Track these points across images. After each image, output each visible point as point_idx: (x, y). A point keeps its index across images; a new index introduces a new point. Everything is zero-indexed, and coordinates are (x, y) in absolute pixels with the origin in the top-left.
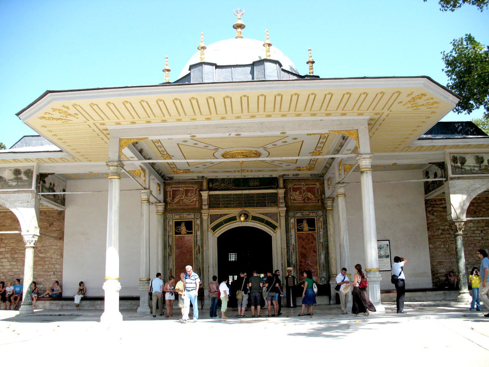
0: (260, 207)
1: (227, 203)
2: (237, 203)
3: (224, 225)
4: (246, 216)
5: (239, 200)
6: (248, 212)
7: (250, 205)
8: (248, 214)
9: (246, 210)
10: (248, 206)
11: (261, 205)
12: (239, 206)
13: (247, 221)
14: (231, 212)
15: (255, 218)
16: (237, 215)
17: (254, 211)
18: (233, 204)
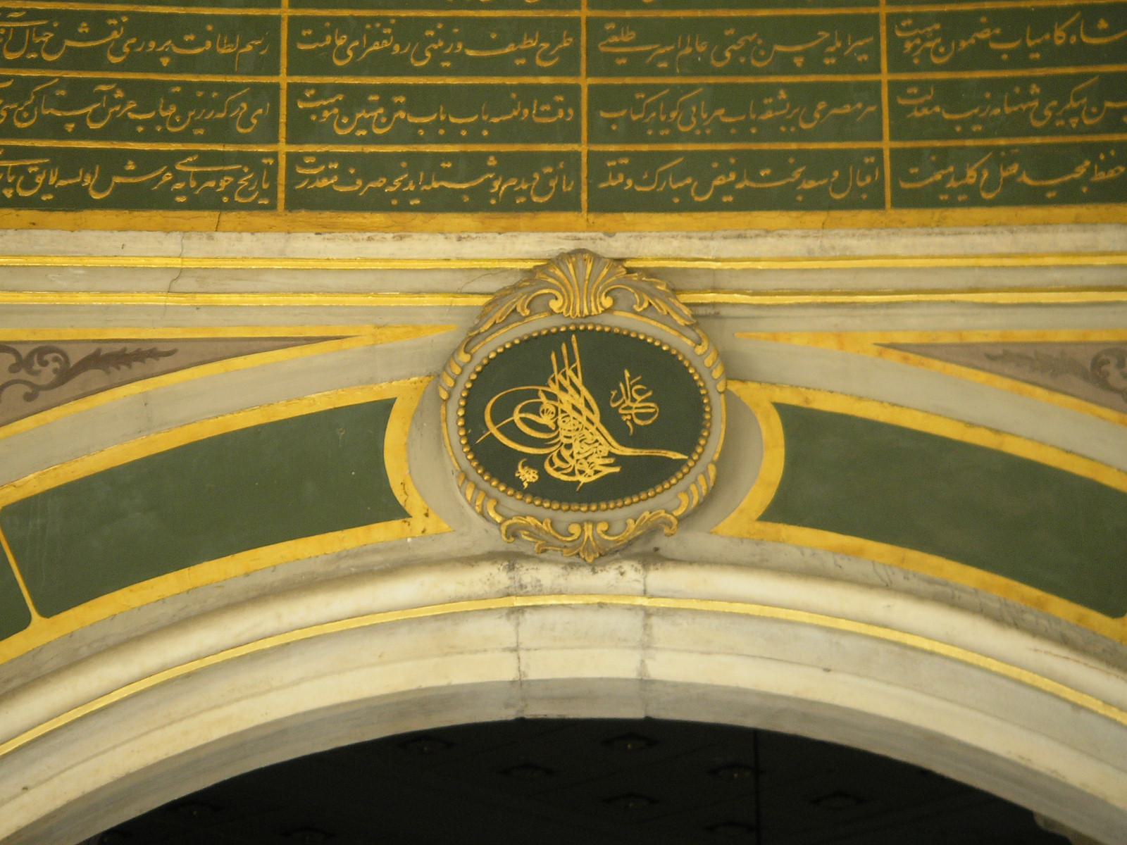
0: (1015, 196)
1: (146, 95)
2: (420, 99)
3: (41, 631)
4: (636, 405)
5: (476, 33)
6: (703, 320)
7: (748, 164)
8: (700, 357)
9: (616, 246)
10: (698, 166)
11: (1047, 162)
12: (475, 164)
13: (652, 558)
14: (236, 312)
15: (864, 484)
16: (403, 390)
17: (839, 299)
18: (302, 128)
